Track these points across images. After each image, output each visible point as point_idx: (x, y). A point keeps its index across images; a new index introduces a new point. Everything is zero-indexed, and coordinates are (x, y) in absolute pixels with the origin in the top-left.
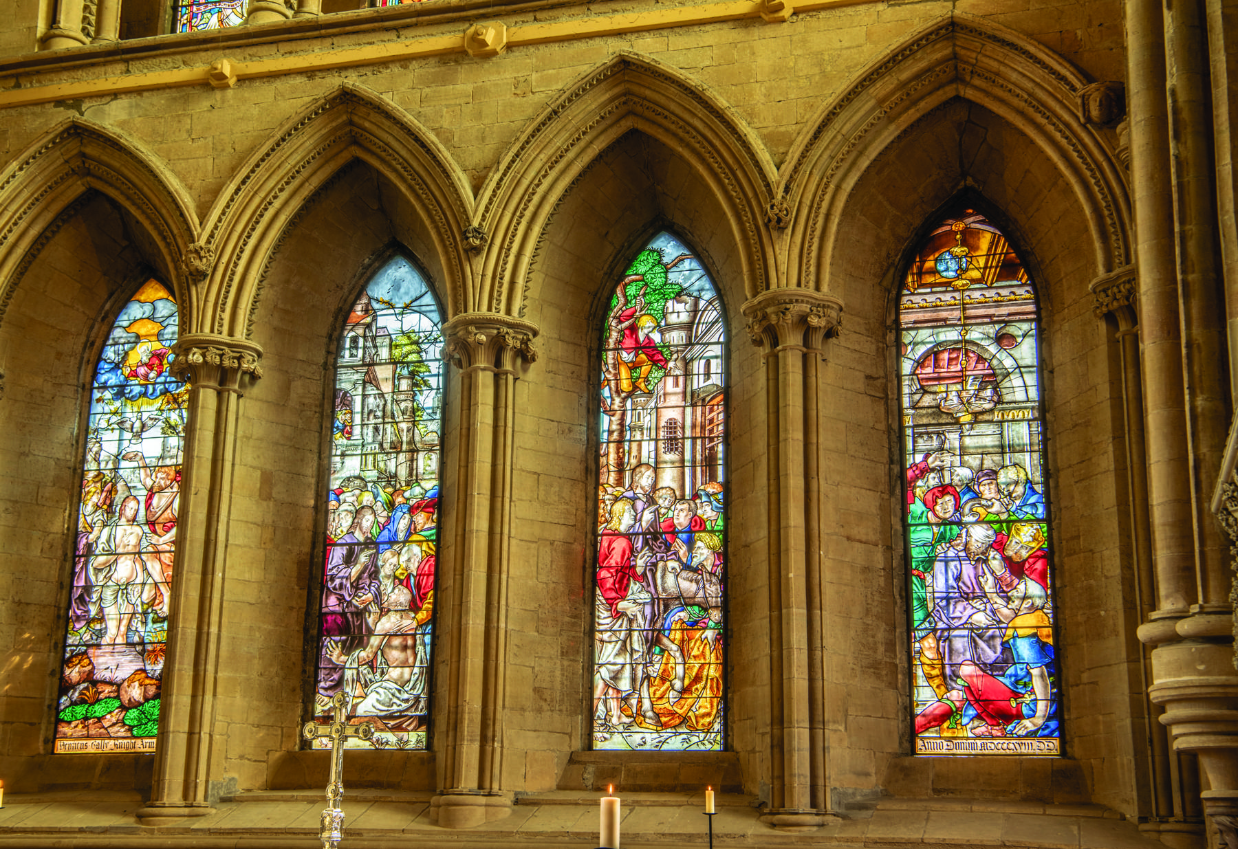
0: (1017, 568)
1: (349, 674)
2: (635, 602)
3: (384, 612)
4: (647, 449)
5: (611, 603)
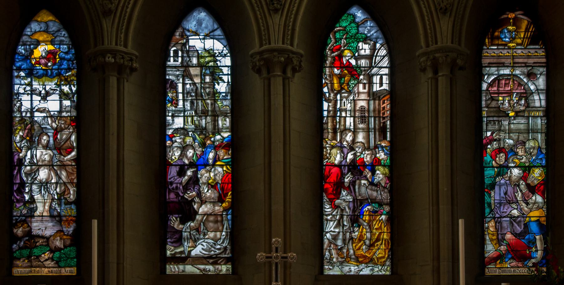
0: (532, 189)
1: (185, 234)
3: (203, 202)
4: (349, 121)
5: (332, 201)
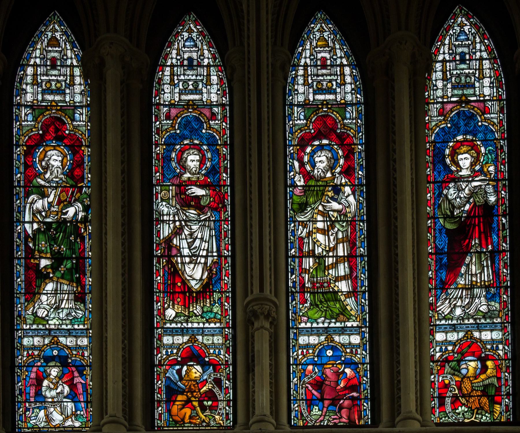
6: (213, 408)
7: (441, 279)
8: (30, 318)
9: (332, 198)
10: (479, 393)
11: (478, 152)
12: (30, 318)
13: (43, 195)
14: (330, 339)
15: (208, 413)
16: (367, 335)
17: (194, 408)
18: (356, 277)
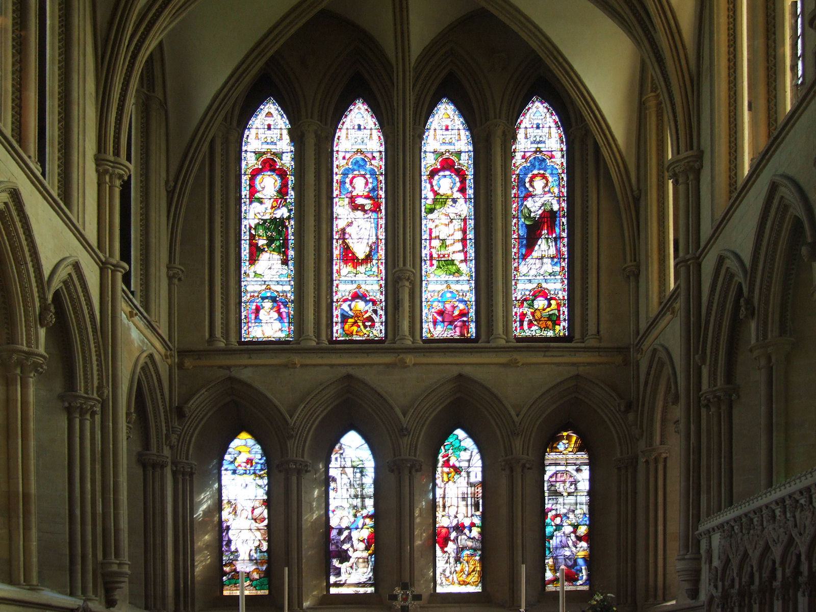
0: (579, 539)
1: (343, 571)
2: (451, 547)
3: (355, 551)
5: (442, 548)
6: (372, 326)
7: (522, 254)
8: (252, 275)
9: (451, 205)
10: (546, 319)
11: (547, 181)
12: (252, 275)
13: (261, 203)
14: (448, 287)
15: (368, 329)
16: (473, 285)
17: (359, 326)
18: (466, 252)
